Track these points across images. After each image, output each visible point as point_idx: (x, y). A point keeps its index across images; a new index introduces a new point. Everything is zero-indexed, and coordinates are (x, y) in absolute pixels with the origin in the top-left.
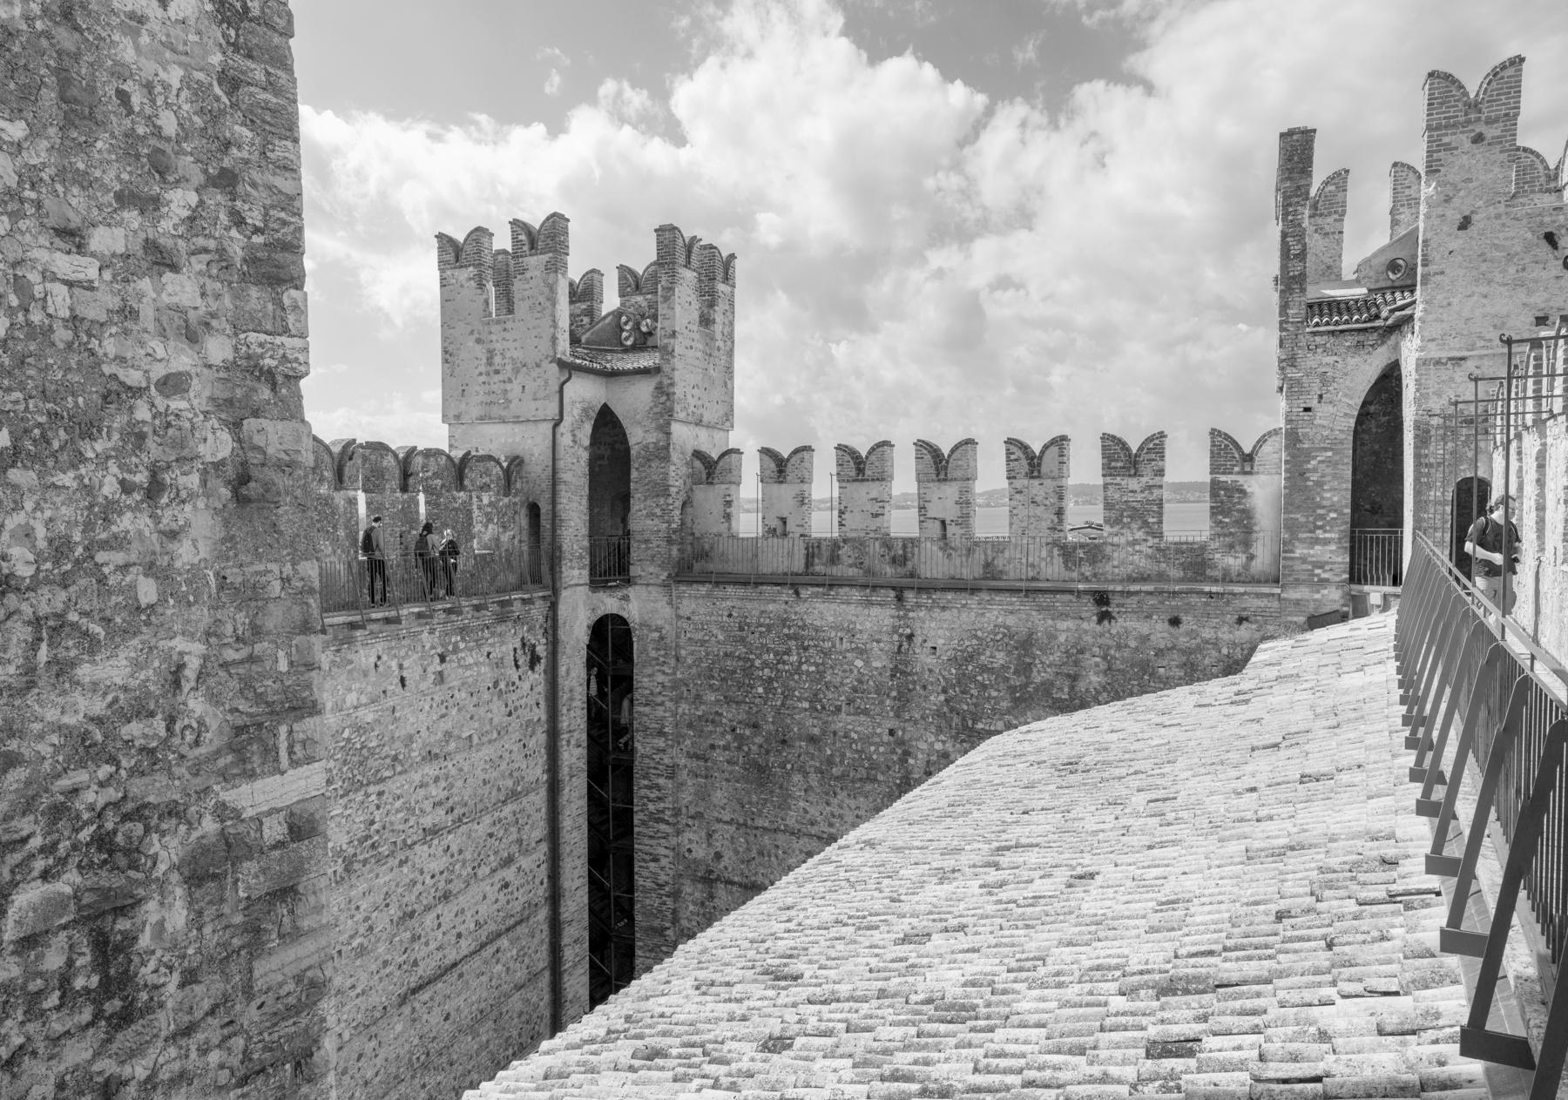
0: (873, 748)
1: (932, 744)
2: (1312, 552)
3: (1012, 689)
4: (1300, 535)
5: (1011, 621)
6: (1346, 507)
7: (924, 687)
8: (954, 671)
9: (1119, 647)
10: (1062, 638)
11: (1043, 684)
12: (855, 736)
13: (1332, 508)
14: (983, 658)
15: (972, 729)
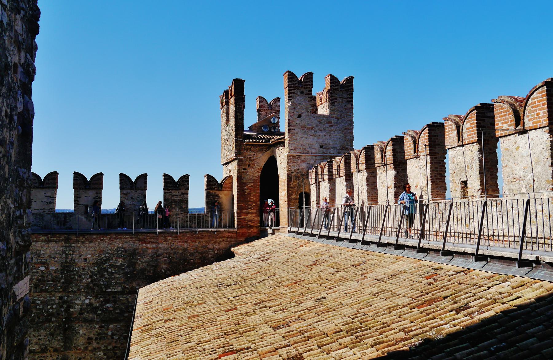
0: (49, 307)
1: (84, 301)
2: (247, 216)
3: (126, 274)
4: (244, 211)
5: (126, 245)
6: (258, 202)
7: (80, 276)
8: (96, 268)
9: (175, 253)
10: (150, 251)
11: (141, 270)
12: (39, 302)
13: (254, 202)
14: (111, 261)
15: (106, 292)
